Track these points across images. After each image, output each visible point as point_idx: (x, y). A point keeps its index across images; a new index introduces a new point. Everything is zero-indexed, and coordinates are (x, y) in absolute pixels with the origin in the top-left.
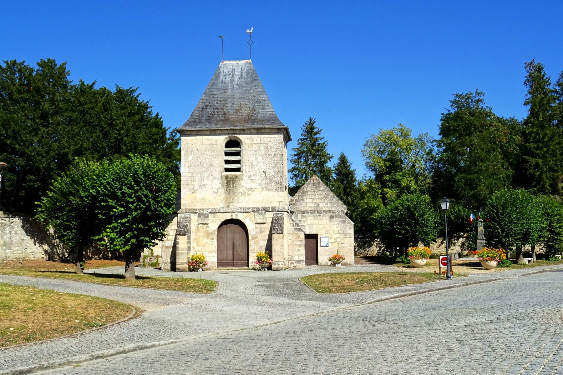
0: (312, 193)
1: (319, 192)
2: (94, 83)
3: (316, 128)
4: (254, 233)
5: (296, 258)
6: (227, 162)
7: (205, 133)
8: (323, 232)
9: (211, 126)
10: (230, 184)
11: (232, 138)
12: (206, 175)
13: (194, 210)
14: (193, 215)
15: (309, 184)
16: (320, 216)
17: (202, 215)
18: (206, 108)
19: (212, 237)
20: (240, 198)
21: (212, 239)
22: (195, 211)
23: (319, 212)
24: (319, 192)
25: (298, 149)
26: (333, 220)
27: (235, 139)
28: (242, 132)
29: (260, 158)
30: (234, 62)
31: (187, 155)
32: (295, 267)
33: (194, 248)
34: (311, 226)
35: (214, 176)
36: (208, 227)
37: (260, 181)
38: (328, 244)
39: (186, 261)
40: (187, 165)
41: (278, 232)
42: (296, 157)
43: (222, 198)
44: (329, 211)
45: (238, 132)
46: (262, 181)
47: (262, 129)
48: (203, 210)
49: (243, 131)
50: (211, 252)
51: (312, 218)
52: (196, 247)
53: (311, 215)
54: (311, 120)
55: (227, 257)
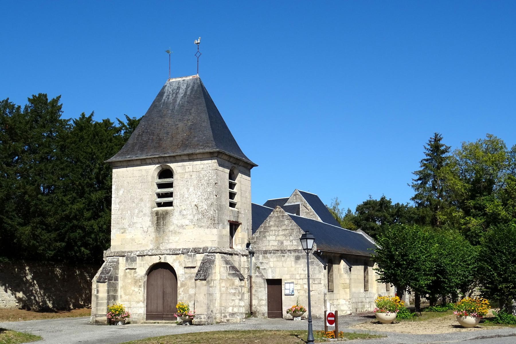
0: (276, 228)
1: (284, 227)
2: (92, 115)
3: (442, 145)
4: (183, 279)
5: (230, 310)
6: (160, 196)
7: (135, 163)
8: (288, 277)
9: (141, 154)
10: (160, 220)
11: (165, 167)
12: (136, 211)
13: (123, 252)
14: (121, 258)
15: (272, 217)
16: (284, 256)
17: (131, 259)
18: (142, 135)
19: (140, 284)
20: (171, 238)
21: (140, 286)
22: (123, 254)
23: (283, 251)
24: (284, 227)
25: (420, 172)
26: (299, 262)
27: (167, 168)
28: (173, 160)
29: (191, 190)
30: (180, 79)
31: (117, 190)
32: (228, 320)
33: (121, 297)
34: (274, 269)
35: (144, 212)
36: (135, 272)
37: (191, 217)
38: (293, 291)
39: (105, 313)
40: (118, 200)
41: (201, 278)
42: (420, 182)
43: (151, 238)
44: (295, 251)
45: (168, 160)
46: (194, 216)
47: (192, 154)
48: (132, 252)
49: (175, 159)
50: (138, 302)
51: (275, 259)
52: (123, 296)
53: (274, 255)
54: (436, 135)
55: (157, 307)
